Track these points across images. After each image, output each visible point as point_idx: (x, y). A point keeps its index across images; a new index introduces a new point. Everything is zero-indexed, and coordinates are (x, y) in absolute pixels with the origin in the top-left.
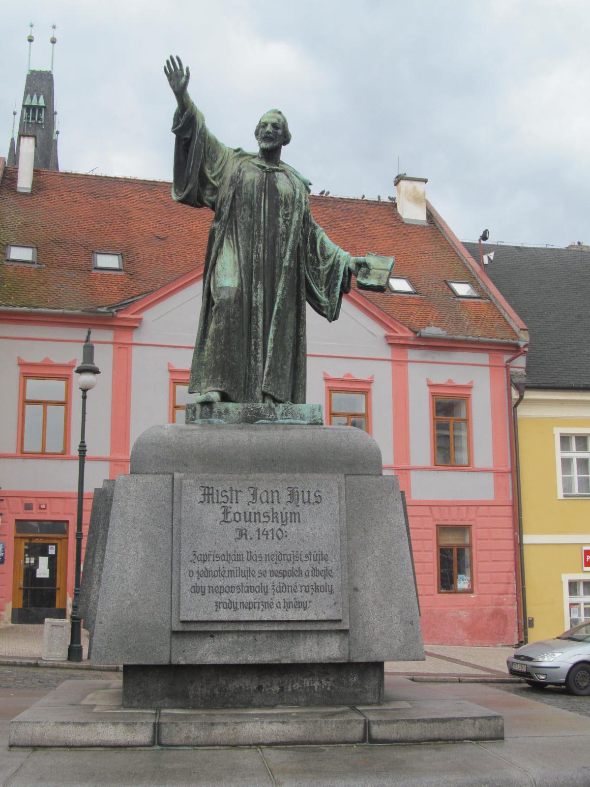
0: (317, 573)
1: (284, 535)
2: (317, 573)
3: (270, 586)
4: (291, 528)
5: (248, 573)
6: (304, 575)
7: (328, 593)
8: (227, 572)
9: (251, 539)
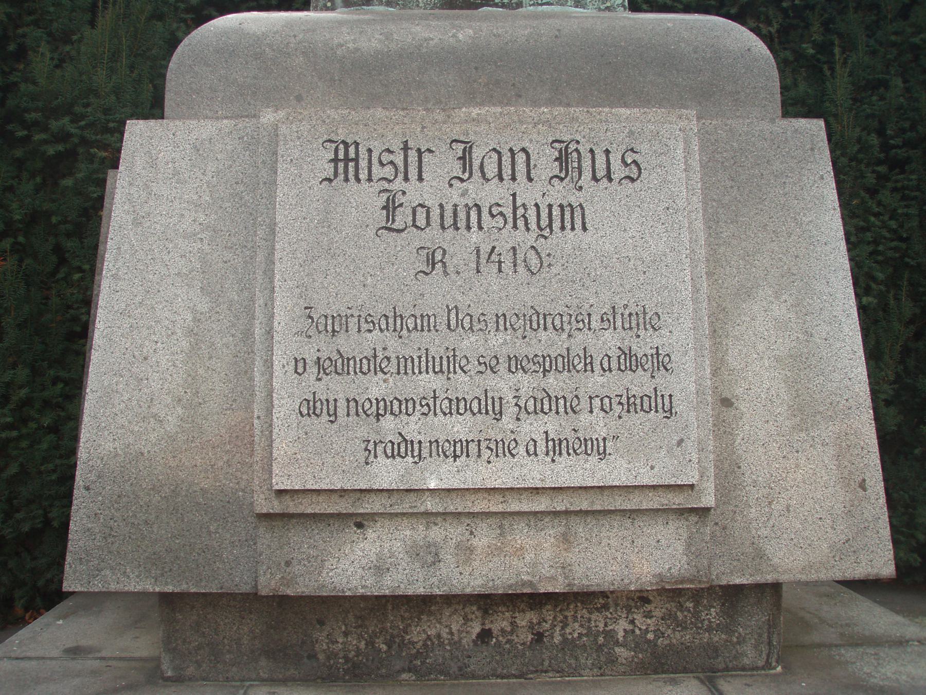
0: (634, 363)
1: (545, 264)
2: (634, 363)
3: (509, 397)
5: (449, 364)
6: (597, 368)
7: (661, 414)
8: (394, 361)
9: (458, 273)
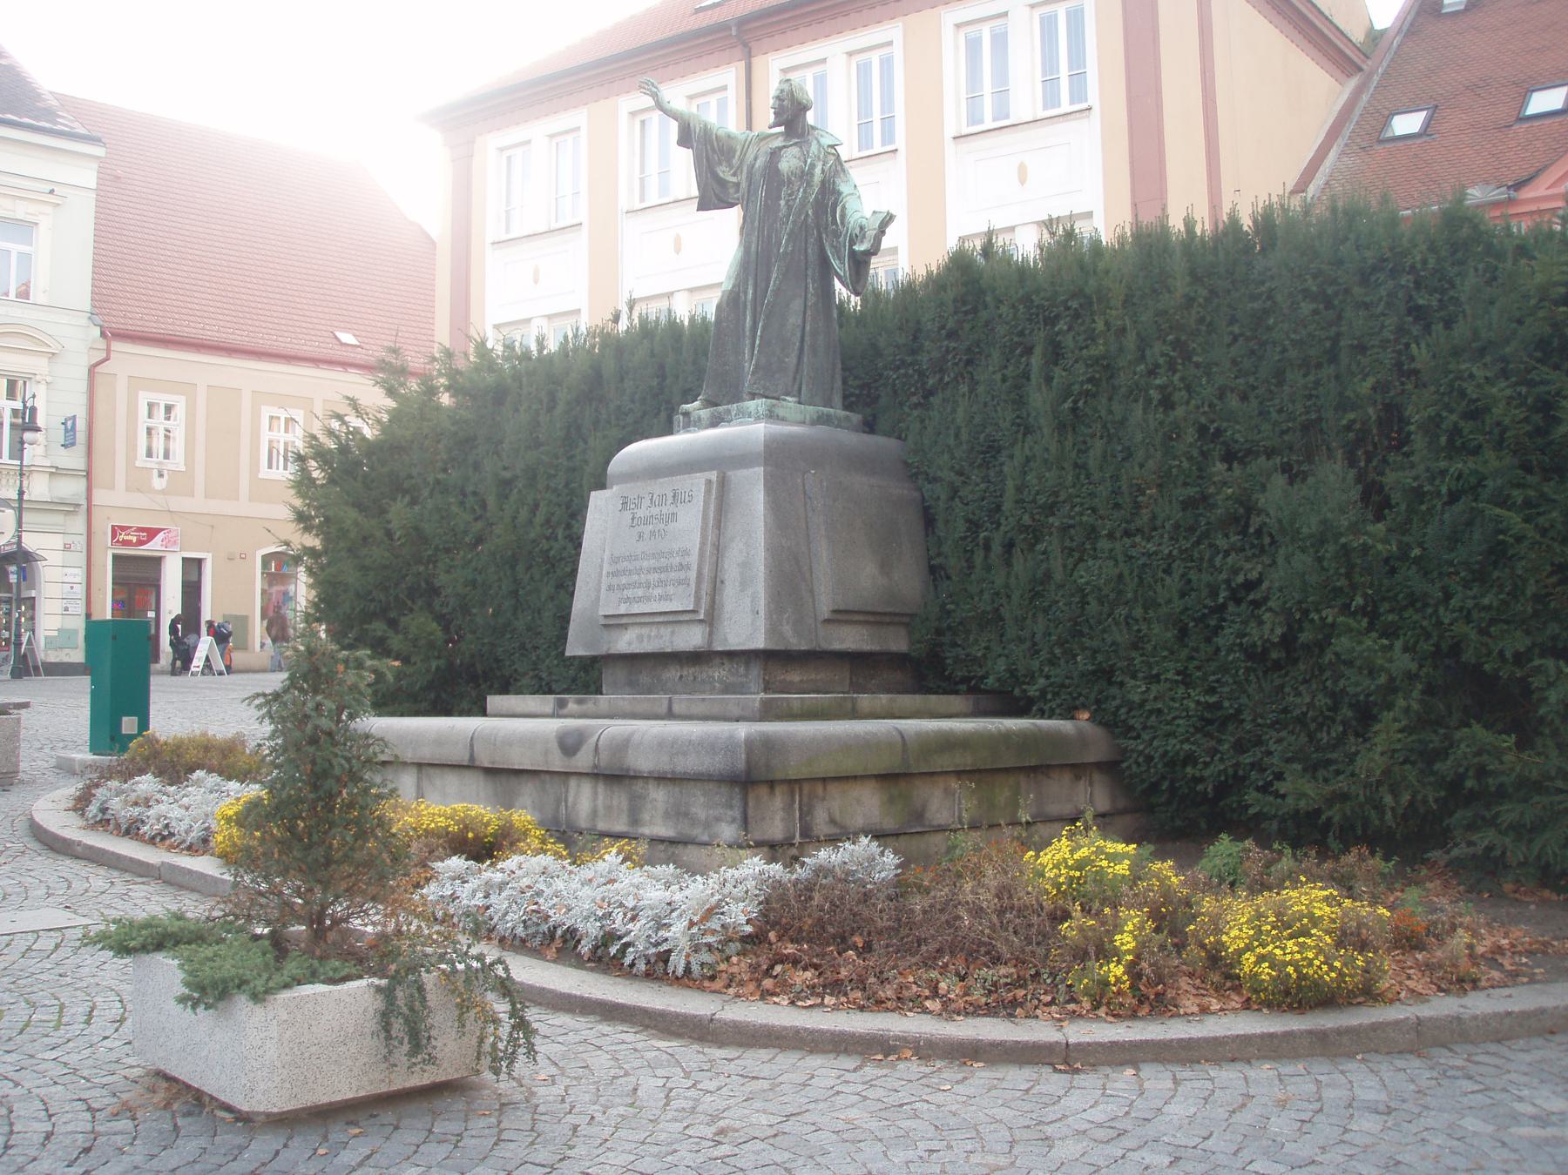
4: (672, 526)
5: (639, 571)
